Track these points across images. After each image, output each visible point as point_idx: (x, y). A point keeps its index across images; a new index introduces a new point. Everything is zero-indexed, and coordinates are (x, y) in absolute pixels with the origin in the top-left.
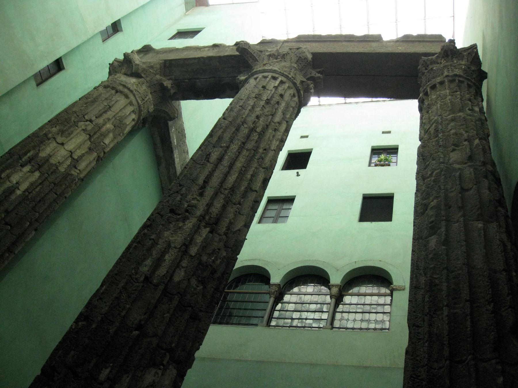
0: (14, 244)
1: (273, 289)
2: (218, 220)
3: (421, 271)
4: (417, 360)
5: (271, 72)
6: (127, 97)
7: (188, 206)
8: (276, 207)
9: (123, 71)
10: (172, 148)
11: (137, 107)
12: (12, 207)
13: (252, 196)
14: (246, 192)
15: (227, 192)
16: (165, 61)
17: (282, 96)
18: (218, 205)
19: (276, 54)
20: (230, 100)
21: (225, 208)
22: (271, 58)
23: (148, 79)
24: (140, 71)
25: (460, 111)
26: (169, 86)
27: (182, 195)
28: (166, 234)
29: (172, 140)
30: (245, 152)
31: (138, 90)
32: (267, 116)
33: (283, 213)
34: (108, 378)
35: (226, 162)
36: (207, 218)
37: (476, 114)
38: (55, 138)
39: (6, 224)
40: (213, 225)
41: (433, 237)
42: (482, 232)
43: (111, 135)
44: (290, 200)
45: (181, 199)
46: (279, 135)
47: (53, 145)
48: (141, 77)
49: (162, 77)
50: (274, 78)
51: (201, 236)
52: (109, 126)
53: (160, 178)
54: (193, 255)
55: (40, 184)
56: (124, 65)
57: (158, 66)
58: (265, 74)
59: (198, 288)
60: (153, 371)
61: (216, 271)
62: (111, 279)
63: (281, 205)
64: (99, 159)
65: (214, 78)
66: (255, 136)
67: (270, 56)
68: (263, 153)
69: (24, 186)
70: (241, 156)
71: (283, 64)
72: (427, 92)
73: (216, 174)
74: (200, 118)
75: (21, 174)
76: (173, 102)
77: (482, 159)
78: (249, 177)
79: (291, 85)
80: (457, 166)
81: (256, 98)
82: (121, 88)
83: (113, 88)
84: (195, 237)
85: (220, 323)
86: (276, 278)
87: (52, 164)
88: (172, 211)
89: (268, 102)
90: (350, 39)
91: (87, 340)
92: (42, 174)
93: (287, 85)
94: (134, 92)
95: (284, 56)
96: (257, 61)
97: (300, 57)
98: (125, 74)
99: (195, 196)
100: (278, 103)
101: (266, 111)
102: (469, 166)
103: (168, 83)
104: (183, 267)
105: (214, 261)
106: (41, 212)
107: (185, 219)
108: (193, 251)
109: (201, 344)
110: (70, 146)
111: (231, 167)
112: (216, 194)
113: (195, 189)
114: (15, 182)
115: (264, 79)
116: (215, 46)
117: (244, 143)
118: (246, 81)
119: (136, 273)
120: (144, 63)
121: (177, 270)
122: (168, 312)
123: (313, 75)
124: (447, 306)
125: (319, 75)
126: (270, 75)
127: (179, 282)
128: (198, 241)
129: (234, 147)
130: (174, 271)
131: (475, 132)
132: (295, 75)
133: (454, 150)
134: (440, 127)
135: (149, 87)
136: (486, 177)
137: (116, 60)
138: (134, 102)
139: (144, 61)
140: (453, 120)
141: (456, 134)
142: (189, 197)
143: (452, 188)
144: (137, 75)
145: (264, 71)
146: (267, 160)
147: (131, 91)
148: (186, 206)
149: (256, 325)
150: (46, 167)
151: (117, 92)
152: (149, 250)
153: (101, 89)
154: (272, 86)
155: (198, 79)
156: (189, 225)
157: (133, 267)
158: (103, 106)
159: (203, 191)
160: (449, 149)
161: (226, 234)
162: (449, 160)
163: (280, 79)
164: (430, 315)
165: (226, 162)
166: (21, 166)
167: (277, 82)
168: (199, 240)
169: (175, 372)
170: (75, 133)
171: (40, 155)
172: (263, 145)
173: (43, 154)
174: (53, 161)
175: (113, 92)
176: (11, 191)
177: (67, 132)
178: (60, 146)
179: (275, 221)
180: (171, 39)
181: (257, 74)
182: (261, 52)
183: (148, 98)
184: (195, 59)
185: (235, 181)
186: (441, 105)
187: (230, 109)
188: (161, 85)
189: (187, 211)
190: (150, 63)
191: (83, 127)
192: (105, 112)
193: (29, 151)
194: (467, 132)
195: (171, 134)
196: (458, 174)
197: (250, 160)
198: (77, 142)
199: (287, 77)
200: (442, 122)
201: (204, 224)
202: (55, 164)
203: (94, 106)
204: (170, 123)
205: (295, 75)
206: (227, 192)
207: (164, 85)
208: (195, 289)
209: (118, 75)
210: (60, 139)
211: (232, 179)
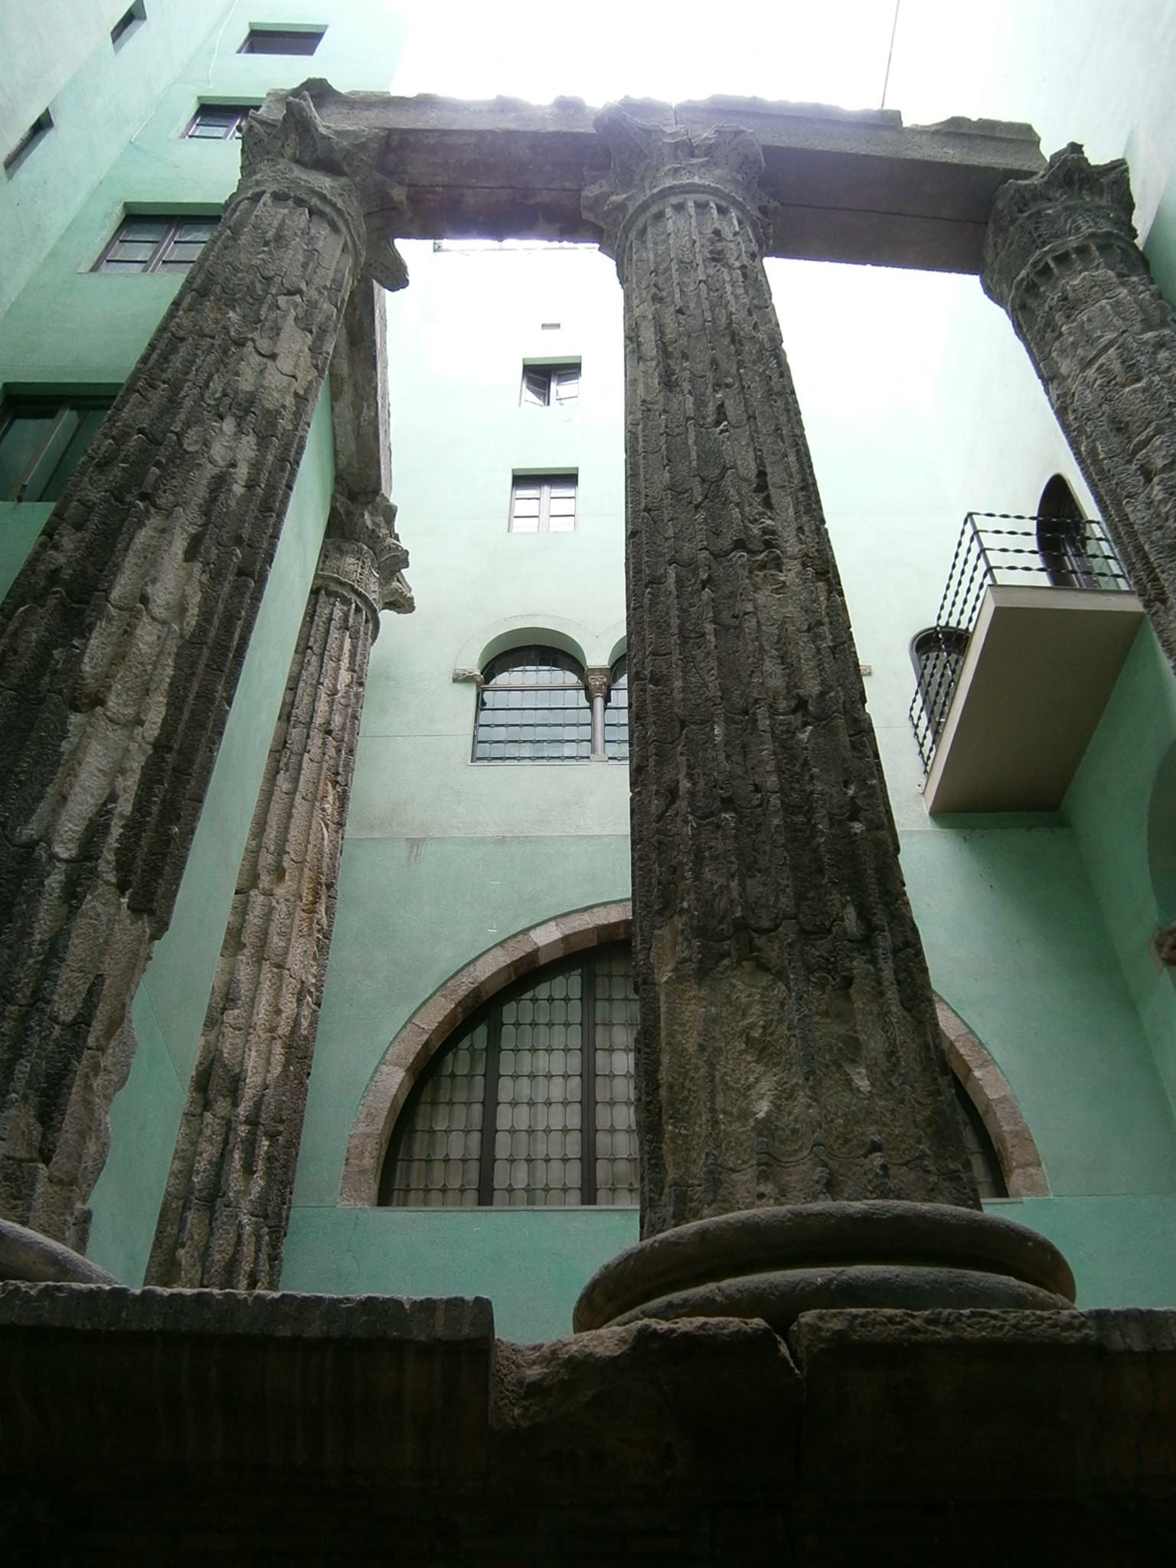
6: (335, 229)
9: (289, 151)
10: (375, 358)
16: (391, 132)
26: (404, 198)
27: (738, 505)
48: (342, 174)
53: (334, 429)
65: (511, 187)
67: (677, 146)
69: (242, 472)
71: (718, 172)
82: (315, 201)
83: (300, 202)
95: (710, 150)
97: (746, 157)
98: (297, 161)
103: (399, 194)
110: (285, 364)
116: (503, 106)
120: (338, 133)
125: (776, 203)
138: (350, 244)
140: (1160, 345)
144: (329, 165)
147: (339, 211)
151: (311, 213)
155: (469, 187)
173: (246, 384)
178: (270, 363)
184: (471, 133)
207: (391, 199)
210: (264, 345)
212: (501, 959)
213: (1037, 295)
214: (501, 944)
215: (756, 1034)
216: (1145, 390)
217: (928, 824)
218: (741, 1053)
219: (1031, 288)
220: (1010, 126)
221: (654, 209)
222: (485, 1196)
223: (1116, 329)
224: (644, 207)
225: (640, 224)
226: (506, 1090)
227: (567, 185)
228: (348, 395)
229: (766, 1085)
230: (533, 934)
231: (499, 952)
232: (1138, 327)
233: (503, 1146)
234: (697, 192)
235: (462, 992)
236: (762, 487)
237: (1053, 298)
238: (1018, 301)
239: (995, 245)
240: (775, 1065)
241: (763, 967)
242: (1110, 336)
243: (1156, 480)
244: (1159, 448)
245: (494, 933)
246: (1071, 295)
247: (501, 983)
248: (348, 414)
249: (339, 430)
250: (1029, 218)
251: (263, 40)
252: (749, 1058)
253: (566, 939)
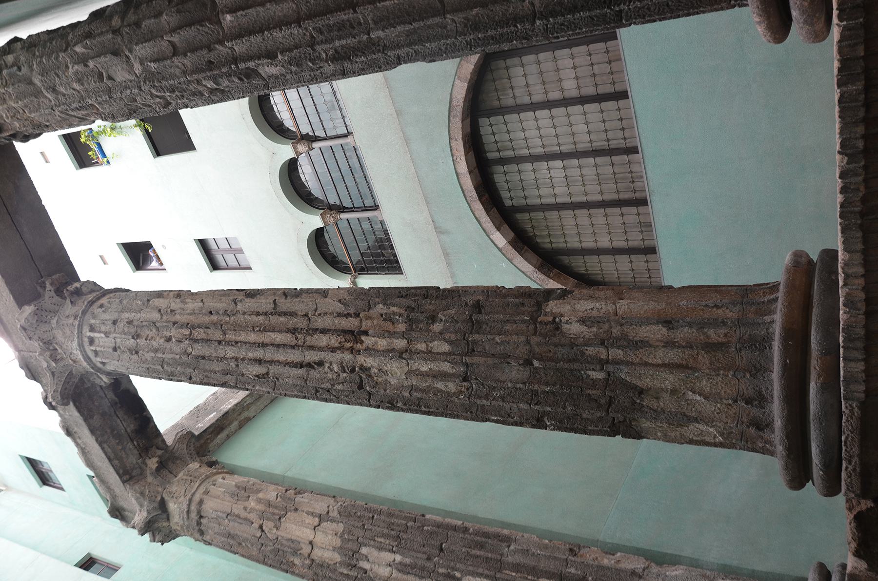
0: (455, 528)
1: (330, 220)
2: (345, 332)
3: (318, 73)
4: (446, 48)
5: (84, 349)
6: (201, 502)
7: (345, 372)
8: (219, 258)
11: (204, 484)
12: (420, 555)
13: (285, 305)
14: (285, 314)
15: (300, 336)
16: (124, 482)
17: (115, 322)
18: (323, 340)
19: (48, 353)
20: (132, 377)
21: (324, 329)
22: (58, 357)
23: (160, 489)
24: (156, 505)
25: (30, 83)
26: (155, 460)
27: (333, 385)
28: (393, 381)
29: (214, 421)
30: (230, 336)
31: (183, 493)
32: (158, 329)
33: (224, 245)
34: (602, 369)
35: (259, 353)
36: (348, 345)
37: (22, 59)
38: (309, 556)
39: (441, 550)
40: (355, 335)
41: (260, 72)
42: (239, 13)
43: (261, 495)
44: (203, 244)
45: (339, 384)
46: (176, 305)
47: (317, 554)
48: (163, 499)
49: (148, 474)
50: (92, 341)
51: (376, 343)
52: (252, 504)
54: (406, 341)
55: (374, 540)
56: (158, 528)
57: (137, 487)
58: (91, 355)
59: (444, 319)
60: (565, 327)
61: (408, 307)
62: (479, 415)
63: (213, 253)
64: (298, 492)
66: (199, 333)
67: (56, 360)
68: (218, 313)
69: (388, 557)
70: (238, 339)
71: (60, 337)
72: (11, 136)
73: (282, 358)
74: (172, 403)
75: (375, 568)
76: (169, 444)
77: (110, 36)
78: (261, 318)
79: (88, 316)
80: (138, 68)
81: (137, 353)
82: (194, 515)
83: (199, 524)
84: (382, 349)
85: (397, 262)
86: (315, 221)
87: (343, 541)
88: (361, 387)
89: (137, 336)
91: (569, 408)
92: (361, 545)
93: (93, 321)
94: (189, 496)
96: (71, 372)
98: (168, 519)
99: (326, 369)
100: (130, 322)
101: (151, 334)
102: (131, 51)
103: (153, 463)
104: (428, 346)
105: (400, 315)
106: (404, 522)
107: (364, 369)
108: (400, 344)
109: (504, 287)
111: (264, 345)
112: (312, 348)
113: (314, 374)
114: (389, 568)
115: (100, 354)
116: (69, 433)
117: (220, 342)
118: (108, 374)
119: (461, 392)
120: (141, 506)
121: (435, 350)
122: (493, 339)
123: (53, 293)
124: (369, 34)
126: (89, 350)
127: (450, 342)
128: (385, 343)
129: (230, 352)
130: (438, 353)
131: (61, 55)
132: (68, 317)
133: (110, 78)
134: (74, 105)
135: (169, 482)
136: (138, 24)
137: (153, 540)
138: (202, 490)
139: (138, 508)
140: (54, 90)
141: (80, 81)
142: (330, 376)
143: (177, 67)
144: (163, 505)
145: (87, 358)
146: (220, 306)
147: (190, 501)
148: (345, 375)
149: (382, 223)
150: (350, 545)
151: (201, 517)
152: (424, 391)
153: (207, 538)
154: (107, 339)
156: (370, 362)
157: (456, 400)
158: (231, 524)
159: (315, 363)
160: (110, 85)
161: (357, 315)
162: (131, 81)
163: (89, 334)
164: (384, 50)
165: (259, 353)
166: (366, 573)
167: (96, 335)
168: (382, 343)
169: (551, 304)
170: (289, 537)
171: (339, 560)
172: (207, 319)
173: (337, 557)
174: (338, 542)
175: (203, 521)
176: (403, 568)
177: (292, 546)
179: (241, 251)
180: (62, 489)
181: (94, 365)
182: (53, 373)
183: (184, 477)
184: (103, 449)
185: (280, 331)
186: (30, 112)
187: (151, 373)
188: (158, 470)
189: (353, 370)
190: (137, 499)
191: (275, 531)
192: (238, 516)
193: (342, 573)
194: (67, 67)
195: (208, 425)
196: (152, 65)
197: (237, 327)
198: (297, 529)
199: (80, 327)
200: (63, 104)
201: (359, 345)
202: (341, 537)
203: (239, 533)
204: (197, 433)
205: (68, 317)
206: (300, 336)
208: (446, 321)
209: (174, 527)
211: (279, 338)
212: (519, 260)
214: (510, 261)
222: (652, 250)
226: (589, 243)
228: (246, 414)
230: (500, 246)
231: (515, 261)
233: (620, 243)
234: (89, 359)
235: (543, 277)
236: (309, 365)
245: (505, 264)
247: (530, 254)
248: (253, 408)
249: (262, 406)
251: (44, 478)
253: (498, 229)
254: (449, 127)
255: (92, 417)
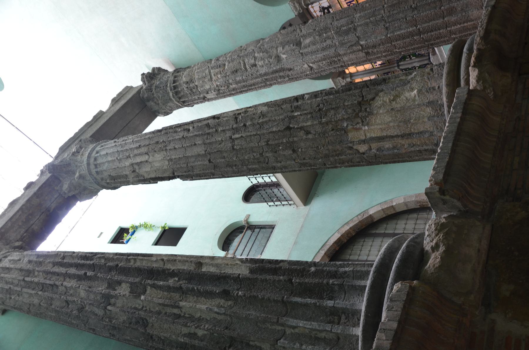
65: (43, 213)
90: (88, 125)
95: (81, 147)
133: (246, 50)
182: (61, 161)
213: (180, 92)
215: (392, 97)
216: (229, 63)
217: (308, 207)
218: (396, 103)
219: (177, 93)
220: (124, 90)
221: (92, 160)
223: (206, 69)
224: (88, 164)
225: (92, 167)
227: (56, 196)
229: (407, 94)
232: (209, 65)
237: (185, 86)
238: (177, 99)
239: (155, 103)
240: (402, 93)
241: (373, 99)
242: (207, 71)
243: (257, 63)
244: (249, 60)
246: (188, 80)
250: (155, 89)
252: (398, 100)
254: (316, 254)
255: (38, 197)
